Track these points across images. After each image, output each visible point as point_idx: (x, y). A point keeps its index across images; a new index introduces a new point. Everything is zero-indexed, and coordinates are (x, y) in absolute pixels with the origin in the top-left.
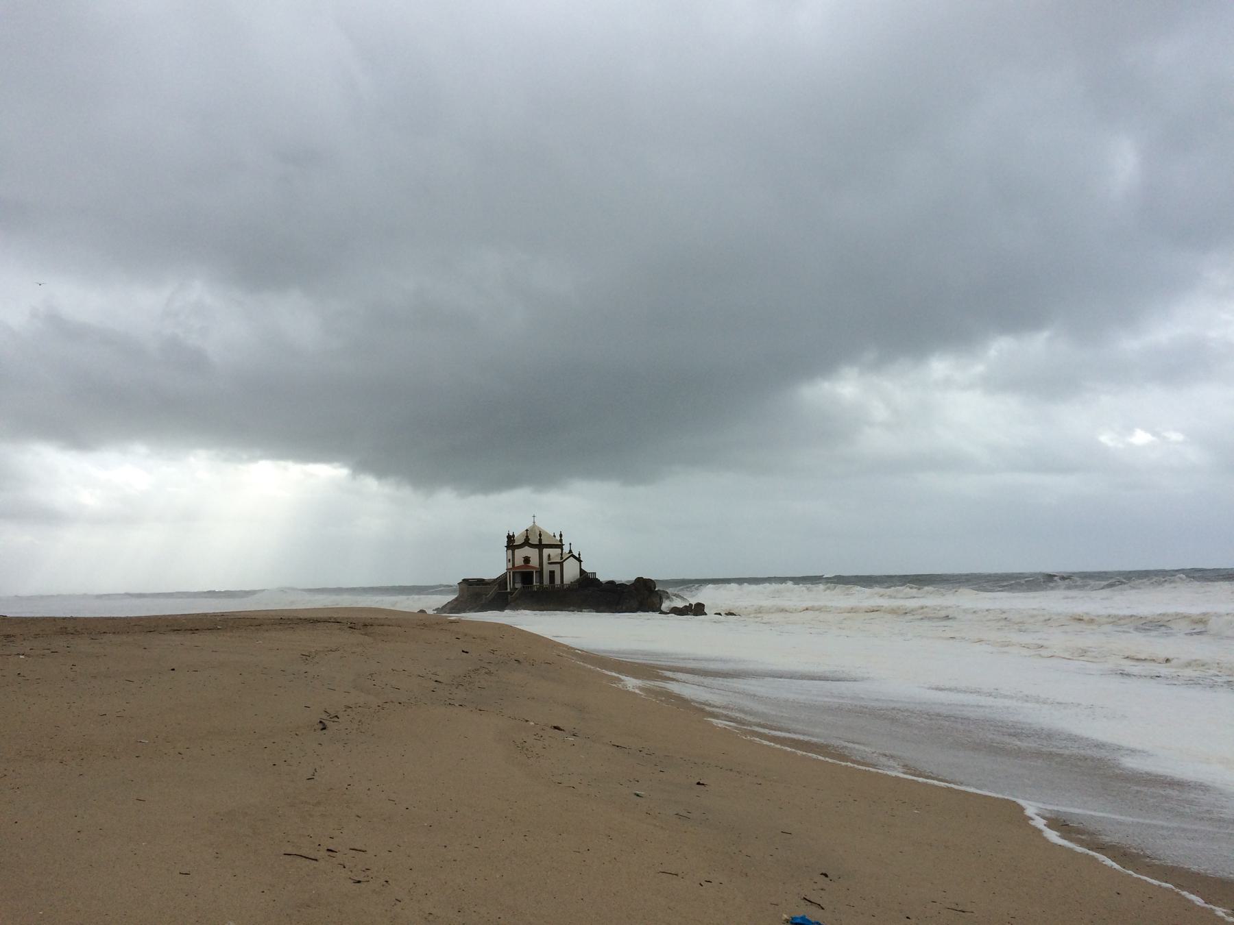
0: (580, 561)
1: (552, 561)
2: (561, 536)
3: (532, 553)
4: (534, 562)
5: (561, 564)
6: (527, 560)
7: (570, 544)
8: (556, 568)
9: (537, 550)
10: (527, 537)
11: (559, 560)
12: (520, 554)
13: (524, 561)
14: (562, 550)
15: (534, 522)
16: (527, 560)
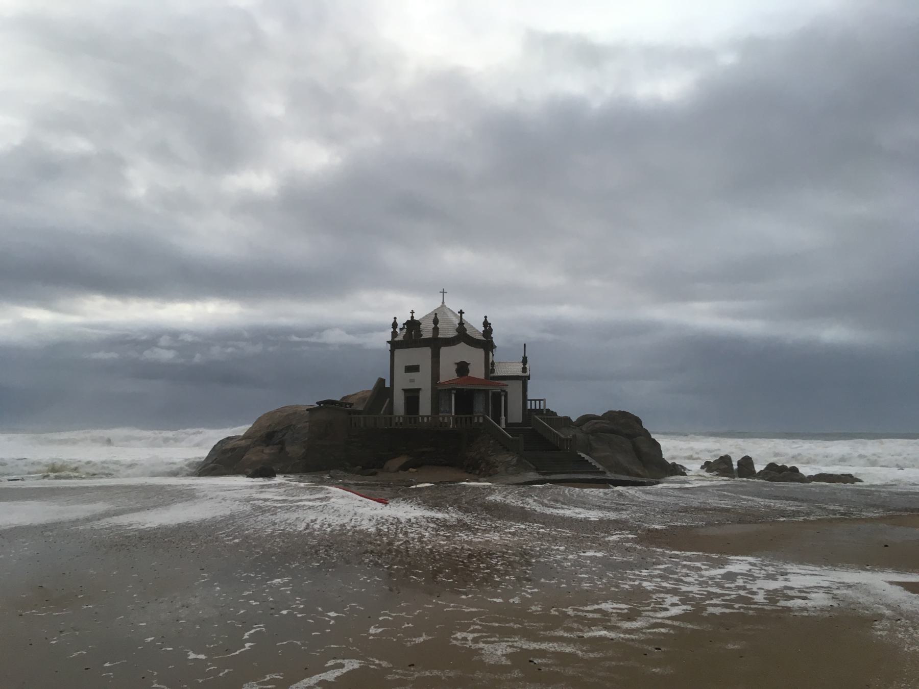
0: (529, 379)
1: (495, 374)
2: (491, 330)
3: (474, 358)
4: (477, 371)
5: (524, 380)
6: (462, 368)
7: (525, 344)
8: (514, 389)
9: (481, 352)
10: (461, 324)
11: (520, 373)
12: (450, 357)
13: (458, 371)
14: (493, 355)
15: (443, 303)
16: (462, 368)
